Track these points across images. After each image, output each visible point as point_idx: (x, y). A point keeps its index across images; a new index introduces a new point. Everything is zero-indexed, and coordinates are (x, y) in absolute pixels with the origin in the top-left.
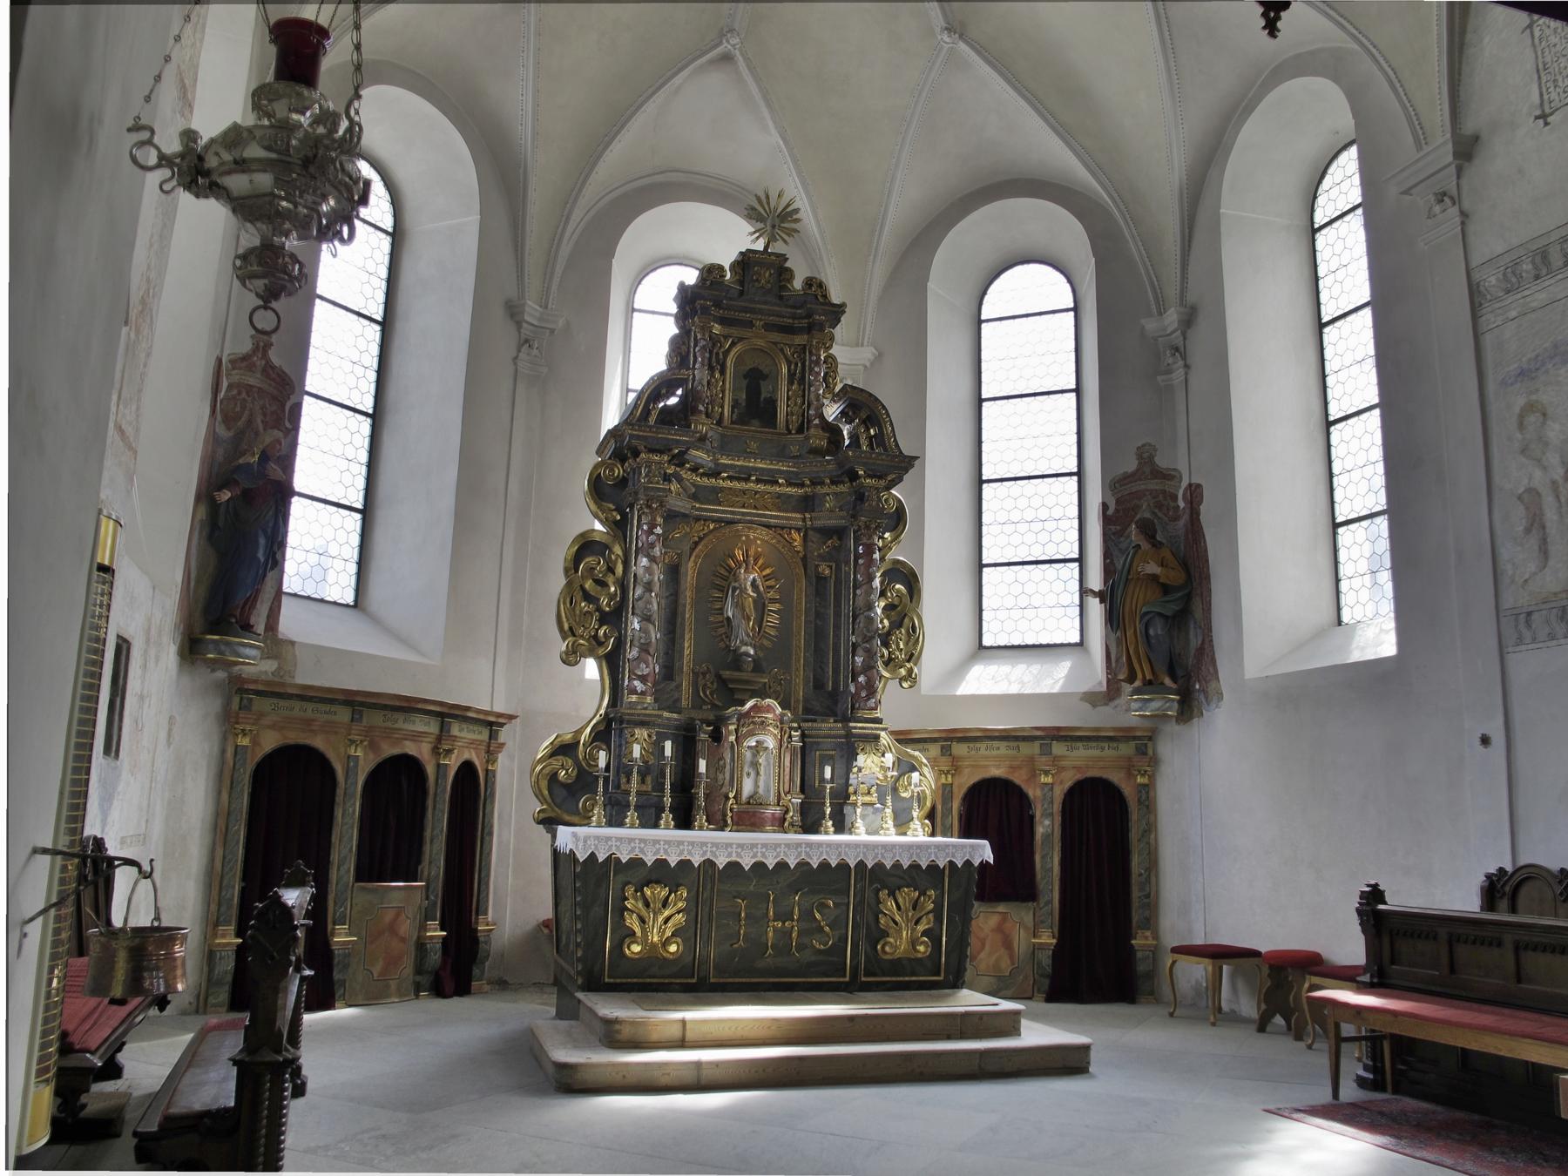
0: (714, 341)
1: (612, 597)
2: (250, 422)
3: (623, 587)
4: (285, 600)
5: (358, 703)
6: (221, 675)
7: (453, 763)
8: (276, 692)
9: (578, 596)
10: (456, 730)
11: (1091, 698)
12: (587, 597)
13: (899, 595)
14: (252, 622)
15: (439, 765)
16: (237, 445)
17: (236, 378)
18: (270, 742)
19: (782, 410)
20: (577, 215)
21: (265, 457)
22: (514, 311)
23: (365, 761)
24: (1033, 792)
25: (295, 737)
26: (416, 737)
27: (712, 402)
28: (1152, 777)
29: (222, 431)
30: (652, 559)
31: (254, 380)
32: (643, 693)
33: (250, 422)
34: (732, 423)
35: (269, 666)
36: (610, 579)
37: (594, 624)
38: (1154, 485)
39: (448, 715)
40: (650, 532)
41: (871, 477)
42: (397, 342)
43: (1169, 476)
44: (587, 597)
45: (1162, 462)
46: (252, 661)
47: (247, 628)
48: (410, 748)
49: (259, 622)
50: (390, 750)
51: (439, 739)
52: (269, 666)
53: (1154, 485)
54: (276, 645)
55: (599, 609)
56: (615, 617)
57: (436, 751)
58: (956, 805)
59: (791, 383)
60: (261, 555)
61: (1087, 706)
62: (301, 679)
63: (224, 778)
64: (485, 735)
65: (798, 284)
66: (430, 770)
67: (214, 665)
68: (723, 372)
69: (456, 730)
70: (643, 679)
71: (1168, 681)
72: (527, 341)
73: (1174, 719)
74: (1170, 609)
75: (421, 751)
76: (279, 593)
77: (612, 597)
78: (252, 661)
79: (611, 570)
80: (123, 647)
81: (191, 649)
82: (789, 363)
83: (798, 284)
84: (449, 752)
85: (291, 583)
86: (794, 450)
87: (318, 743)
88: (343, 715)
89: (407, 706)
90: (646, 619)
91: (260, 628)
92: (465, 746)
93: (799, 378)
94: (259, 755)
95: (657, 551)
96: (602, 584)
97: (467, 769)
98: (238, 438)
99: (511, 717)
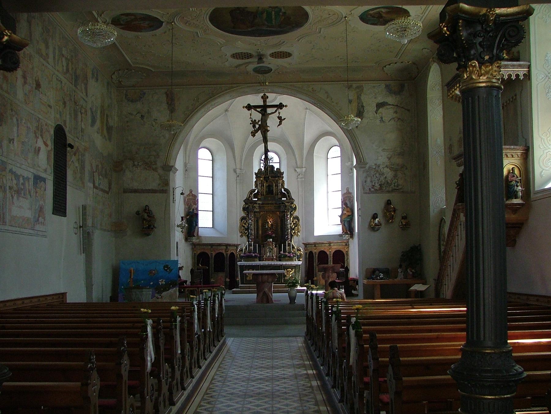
0: (262, 181)
1: (247, 226)
2: (191, 204)
3: (248, 224)
4: (199, 228)
5: (212, 245)
6: (191, 243)
7: (229, 253)
8: (199, 245)
9: (242, 226)
10: (229, 247)
11: (340, 236)
12: (244, 227)
13: (296, 221)
14: (194, 234)
15: (226, 254)
16: (189, 208)
17: (188, 198)
18: (199, 252)
19: (274, 191)
20: (245, 150)
21: (193, 210)
22: (235, 171)
23: (214, 254)
24: (328, 253)
25: (202, 251)
26: (222, 249)
27: (262, 192)
28: (348, 250)
29: (187, 207)
30: (251, 220)
31: (191, 197)
32: (251, 241)
33: (191, 204)
34: (266, 195)
35: (198, 241)
36: (247, 223)
37: (245, 231)
38: (349, 195)
39: (227, 245)
40: (251, 216)
41: (287, 203)
42: (215, 180)
43: (350, 193)
44: (244, 227)
45: (350, 191)
46: (194, 240)
47: (194, 236)
48: (221, 251)
49: (195, 234)
50: (217, 252)
51: (226, 249)
52: (198, 241)
53: (349, 195)
54: (199, 237)
55: (245, 228)
56: (247, 229)
57: (226, 251)
58: (317, 255)
59: (275, 187)
60: (194, 225)
61: (339, 237)
62: (203, 242)
63: (193, 257)
64: (236, 247)
65: (275, 170)
66: (225, 254)
67: (190, 241)
68: (264, 186)
69: (229, 247)
70: (251, 239)
71: (349, 232)
72: (238, 176)
73: (351, 239)
74: (348, 220)
75: (224, 252)
76: (198, 228)
77: (247, 226)
78: (194, 240)
79: (247, 222)
80: (177, 243)
81: (186, 240)
82: (275, 183)
83: (275, 170)
84: (228, 251)
85: (200, 225)
86: (276, 198)
87: (207, 251)
88: (210, 247)
89: (220, 245)
90: (251, 230)
91: (196, 235)
92: (231, 250)
93: (277, 186)
94: (197, 254)
95: (252, 219)
96: (245, 224)
97: (232, 254)
98: (189, 208)
99: (240, 244)
